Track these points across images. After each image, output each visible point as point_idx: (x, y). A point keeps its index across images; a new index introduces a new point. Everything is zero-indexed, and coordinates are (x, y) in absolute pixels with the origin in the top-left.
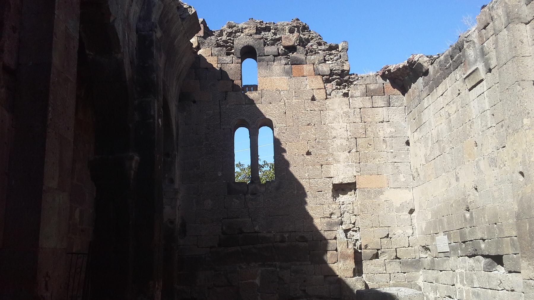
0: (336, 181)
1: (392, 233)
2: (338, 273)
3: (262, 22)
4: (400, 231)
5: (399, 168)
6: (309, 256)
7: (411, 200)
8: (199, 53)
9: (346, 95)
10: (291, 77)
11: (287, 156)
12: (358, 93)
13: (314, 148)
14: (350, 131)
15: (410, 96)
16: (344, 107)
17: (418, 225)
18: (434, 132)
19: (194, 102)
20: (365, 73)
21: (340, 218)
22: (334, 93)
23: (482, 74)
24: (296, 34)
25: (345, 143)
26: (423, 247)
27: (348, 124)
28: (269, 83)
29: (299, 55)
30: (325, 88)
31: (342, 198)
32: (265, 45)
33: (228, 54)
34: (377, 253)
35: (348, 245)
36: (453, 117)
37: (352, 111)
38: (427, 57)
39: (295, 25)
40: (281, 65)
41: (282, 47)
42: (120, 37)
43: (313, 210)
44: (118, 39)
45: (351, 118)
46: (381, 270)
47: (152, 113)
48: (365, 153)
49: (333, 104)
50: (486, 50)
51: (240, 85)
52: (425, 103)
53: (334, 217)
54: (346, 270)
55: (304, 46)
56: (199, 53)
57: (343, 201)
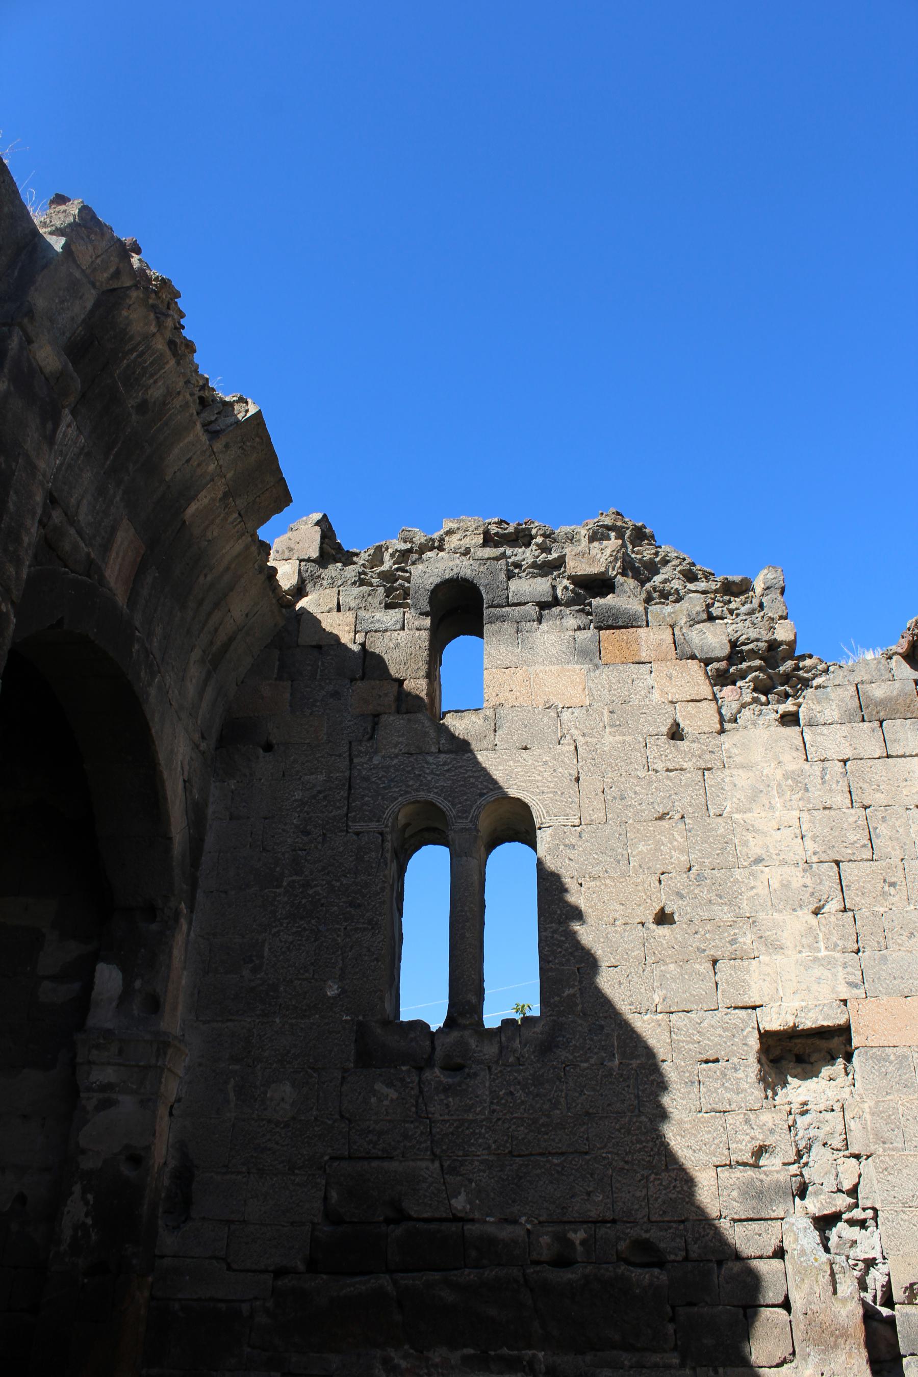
0: (774, 1022)
6: (671, 1328)
8: (302, 603)
9: (790, 719)
10: (597, 666)
11: (587, 934)
12: (831, 712)
13: (682, 897)
14: (814, 839)
16: (786, 757)
19: (268, 748)
21: (794, 1169)
22: (746, 713)
24: (613, 543)
25: (798, 878)
27: (805, 816)
28: (530, 703)
30: (715, 699)
31: (797, 1090)
32: (509, 578)
35: (834, 1283)
37: (817, 768)
41: (566, 582)
43: (683, 1133)
48: (874, 914)
51: (423, 695)
56: (298, 607)
57: (802, 1099)
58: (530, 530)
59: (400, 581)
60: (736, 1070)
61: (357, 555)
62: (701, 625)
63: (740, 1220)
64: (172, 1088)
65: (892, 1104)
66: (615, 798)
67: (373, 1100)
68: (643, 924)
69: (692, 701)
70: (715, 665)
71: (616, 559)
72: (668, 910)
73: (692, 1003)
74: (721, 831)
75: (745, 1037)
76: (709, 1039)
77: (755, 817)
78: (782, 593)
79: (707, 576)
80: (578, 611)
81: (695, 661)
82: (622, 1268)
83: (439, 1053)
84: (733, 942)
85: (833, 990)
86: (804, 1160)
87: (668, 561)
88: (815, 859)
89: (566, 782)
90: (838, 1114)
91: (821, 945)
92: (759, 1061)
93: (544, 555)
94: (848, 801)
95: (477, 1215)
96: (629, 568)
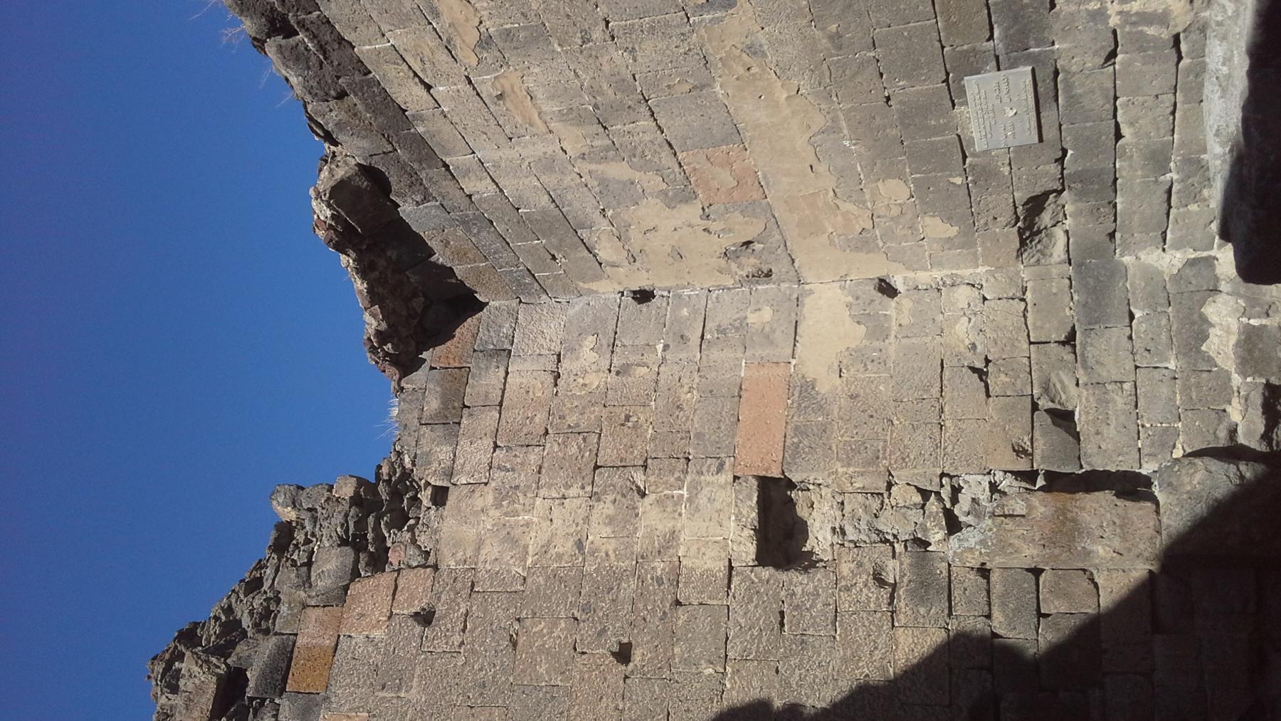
0: (747, 550)
1: (969, 355)
2: (1139, 570)
4: (962, 327)
5: (725, 323)
9: (440, 496)
10: (326, 699)
13: (604, 630)
14: (568, 487)
16: (479, 503)
17: (940, 265)
21: (899, 548)
22: (423, 540)
24: (188, 665)
25: (606, 508)
26: (1023, 243)
27: (542, 492)
31: (820, 539)
34: (1050, 412)
37: (498, 475)
43: (855, 658)
45: (522, 480)
46: (1120, 401)
48: (653, 439)
49: (458, 544)
52: (479, 186)
53: (892, 570)
54: (1124, 527)
57: (829, 536)
60: (794, 594)
62: (312, 573)
63: (950, 608)
65: (841, 445)
66: (481, 694)
68: (626, 677)
69: (394, 594)
70: (361, 566)
72: (616, 648)
73: (718, 632)
75: (760, 580)
76: (758, 619)
78: (303, 489)
79: (260, 566)
80: (255, 716)
81: (351, 587)
84: (659, 581)
85: (723, 487)
86: (890, 538)
87: (230, 606)
88: (589, 488)
94: (537, 449)
96: (223, 651)
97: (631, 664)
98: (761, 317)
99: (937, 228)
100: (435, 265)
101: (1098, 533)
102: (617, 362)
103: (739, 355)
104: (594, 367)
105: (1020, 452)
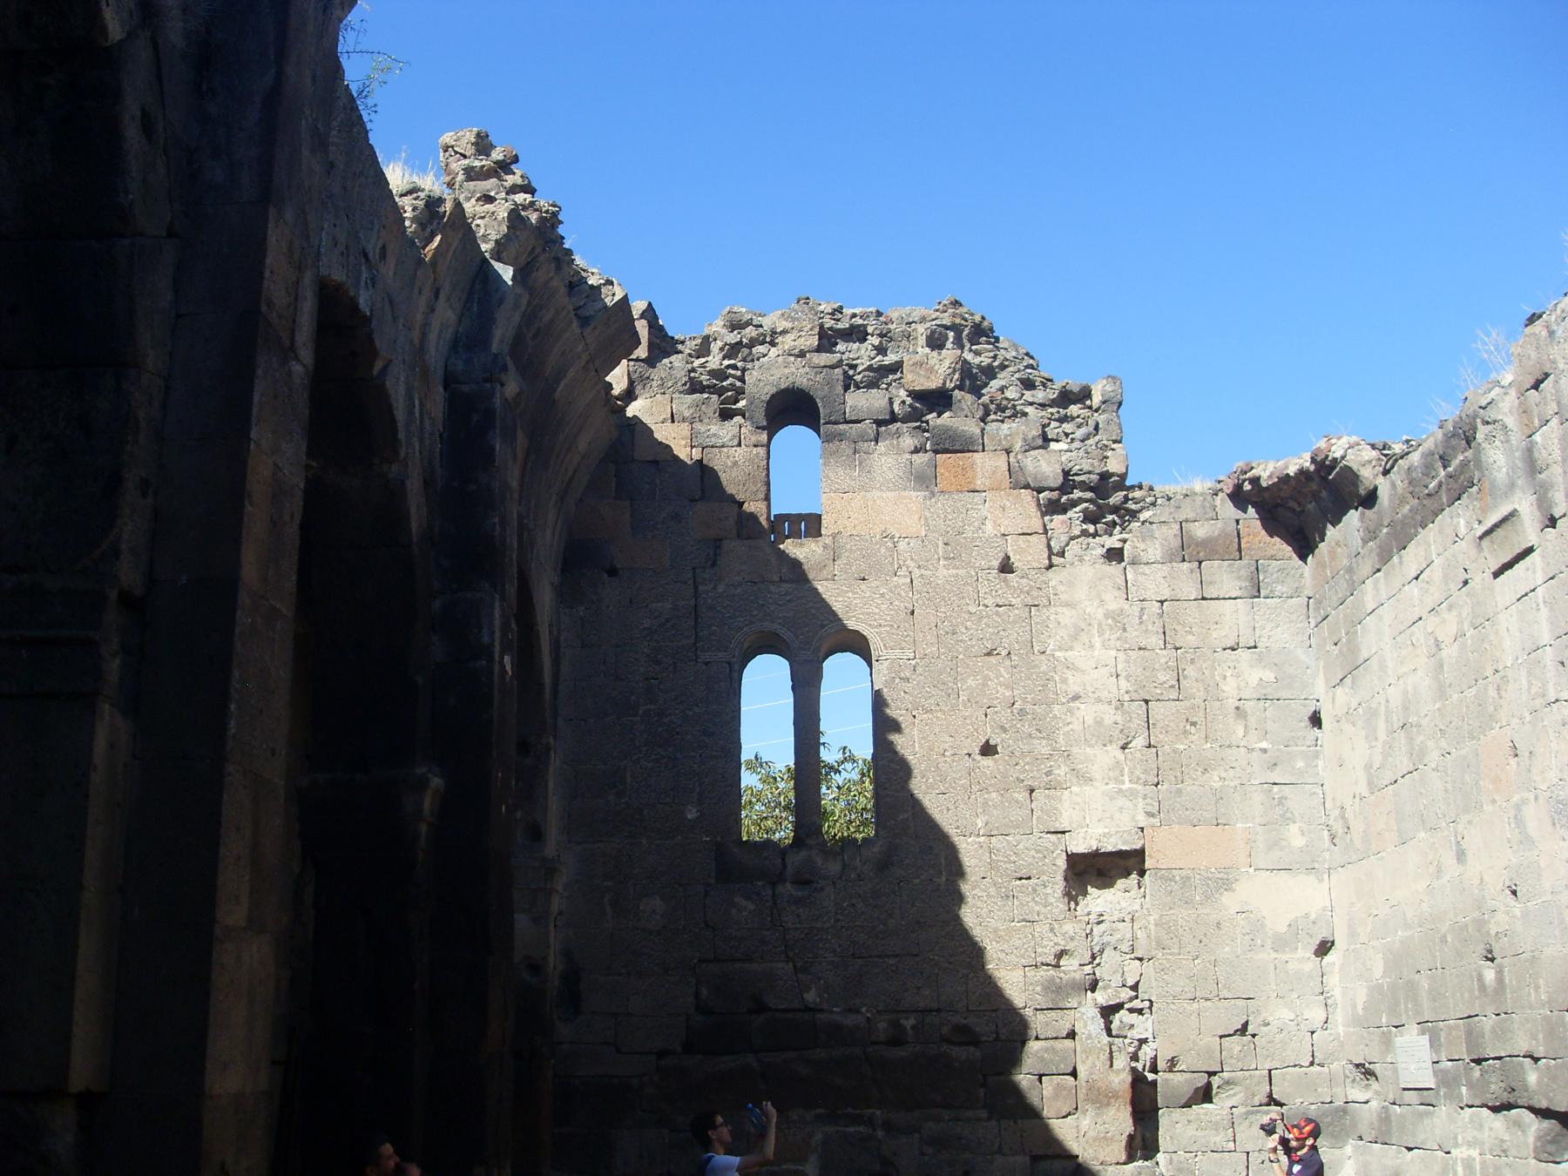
0: (1080, 846)
1: (1259, 1020)
3: (839, 310)
6: (982, 1092)
7: (1324, 909)
8: (632, 410)
9: (1115, 555)
12: (1153, 551)
13: (1005, 730)
14: (1127, 678)
15: (1321, 565)
16: (1108, 597)
18: (1394, 694)
19: (613, 572)
20: (1177, 482)
21: (1088, 969)
22: (1074, 549)
23: (1529, 530)
25: (1110, 716)
26: (1357, 1066)
27: (1121, 656)
29: (960, 420)
30: (1046, 532)
31: (1098, 900)
32: (846, 388)
33: (726, 415)
34: (1209, 1086)
36: (1450, 652)
37: (1136, 609)
38: (1373, 447)
39: (947, 322)
40: (900, 451)
41: (903, 393)
42: (400, 415)
44: (393, 421)
45: (1133, 634)
46: (1220, 1139)
47: (486, 639)
48: (1175, 751)
50: (1541, 455)
52: (1370, 593)
54: (1105, 1140)
55: (976, 391)
57: (1099, 909)
58: (865, 326)
59: (730, 380)
61: (683, 342)
64: (556, 904)
67: (734, 911)
71: (954, 371)
72: (992, 742)
74: (1043, 668)
77: (1076, 655)
82: (945, 1047)
83: (790, 870)
85: (1133, 819)
88: (1127, 698)
89: (903, 615)
90: (1128, 924)
91: (1126, 778)
92: (1065, 879)
93: (879, 358)
95: (825, 1006)
97: (979, 758)
98: (1295, 837)
99: (1361, 997)
100: (1325, 528)
101: (1099, 1121)
102: (1248, 706)
103: (1258, 820)
104: (1243, 684)
105: (1173, 1062)
